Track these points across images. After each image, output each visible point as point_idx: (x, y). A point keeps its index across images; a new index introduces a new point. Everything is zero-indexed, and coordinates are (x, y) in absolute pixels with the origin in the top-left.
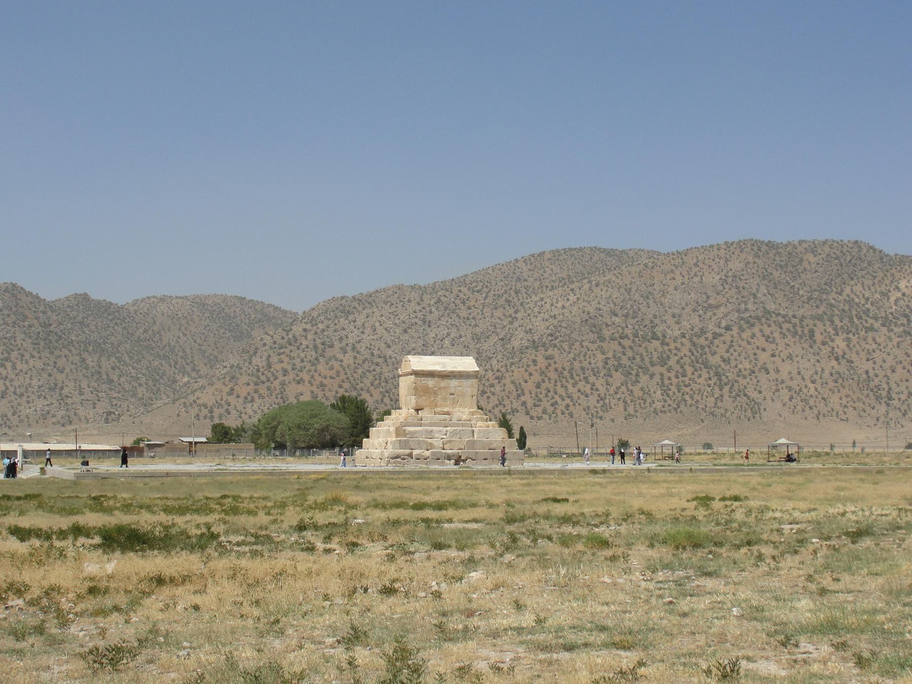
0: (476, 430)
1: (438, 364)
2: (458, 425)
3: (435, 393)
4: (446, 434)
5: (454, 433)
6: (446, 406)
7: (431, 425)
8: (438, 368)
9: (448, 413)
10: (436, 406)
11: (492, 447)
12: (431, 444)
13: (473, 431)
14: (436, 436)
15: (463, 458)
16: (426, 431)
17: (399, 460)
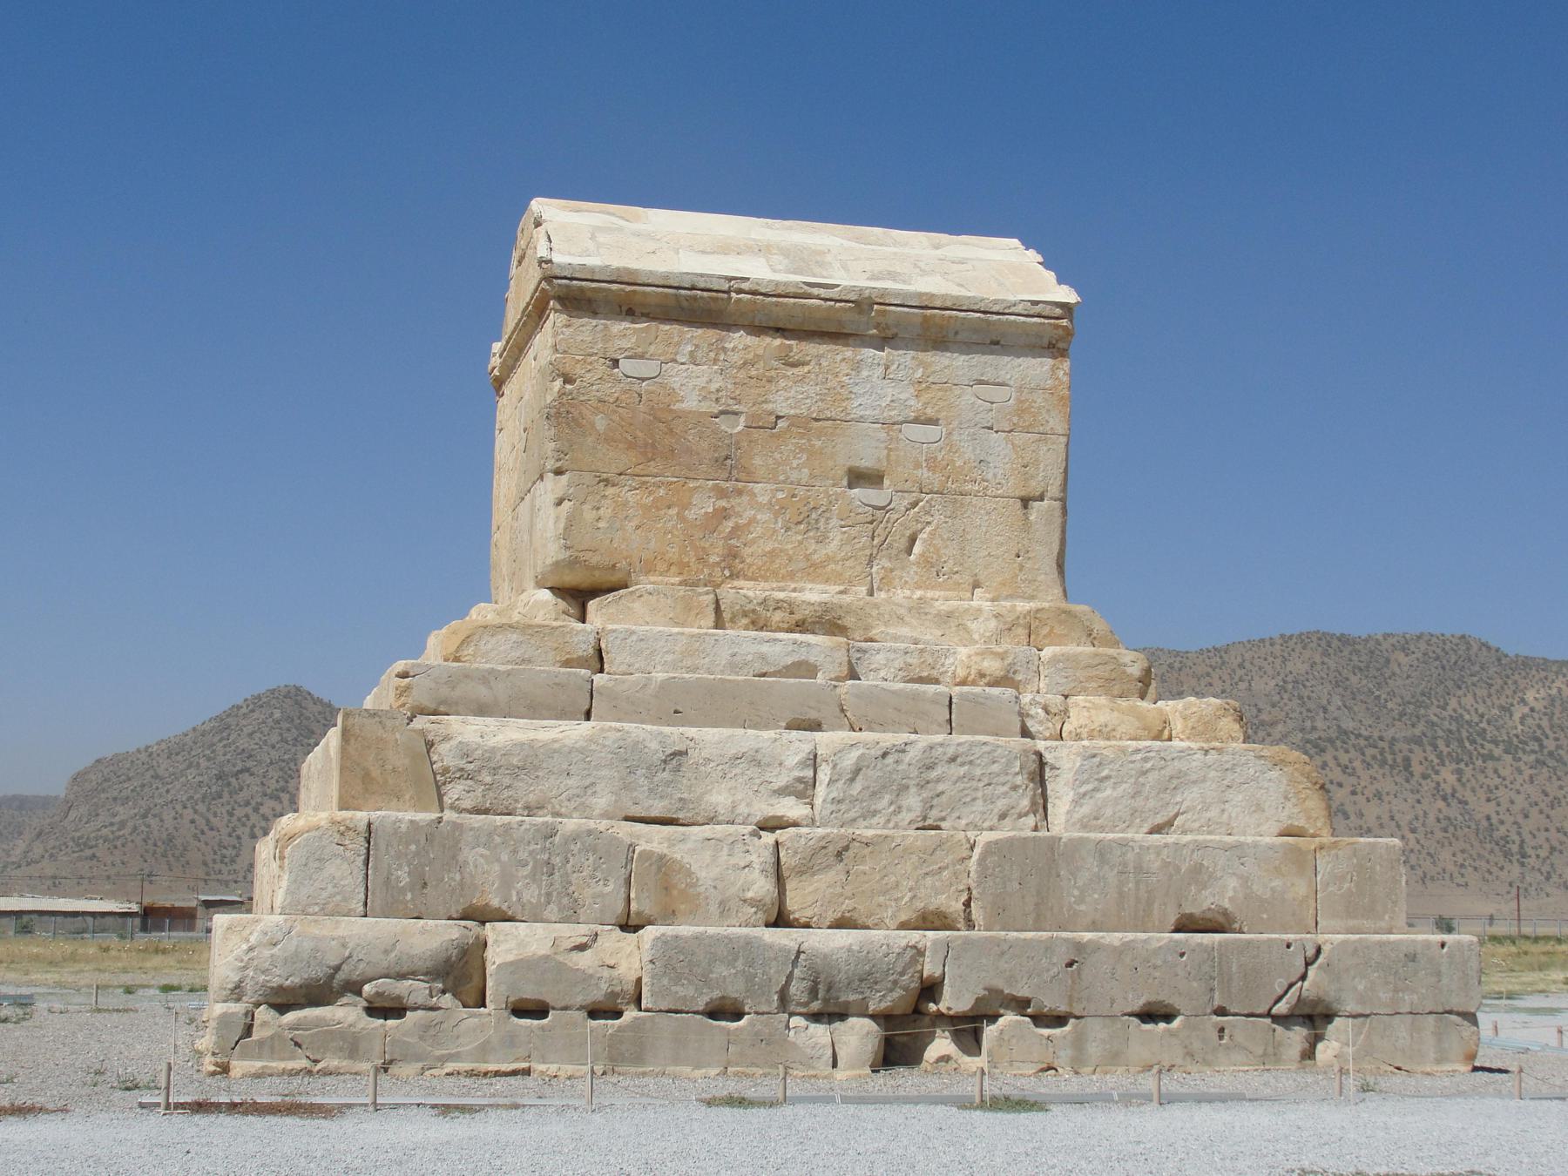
0: (1065, 759)
1: (763, 250)
2: (908, 715)
3: (730, 465)
4: (803, 789)
5: (876, 781)
6: (815, 571)
7: (675, 705)
8: (759, 271)
9: (828, 622)
10: (733, 565)
11: (1203, 902)
12: (663, 866)
13: (1039, 772)
14: (719, 798)
15: (953, 1001)
16: (628, 759)
17: (346, 1014)
